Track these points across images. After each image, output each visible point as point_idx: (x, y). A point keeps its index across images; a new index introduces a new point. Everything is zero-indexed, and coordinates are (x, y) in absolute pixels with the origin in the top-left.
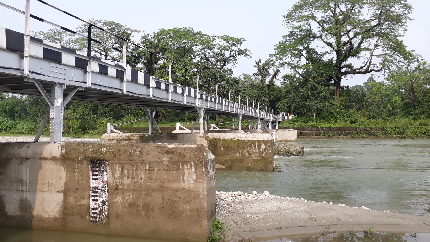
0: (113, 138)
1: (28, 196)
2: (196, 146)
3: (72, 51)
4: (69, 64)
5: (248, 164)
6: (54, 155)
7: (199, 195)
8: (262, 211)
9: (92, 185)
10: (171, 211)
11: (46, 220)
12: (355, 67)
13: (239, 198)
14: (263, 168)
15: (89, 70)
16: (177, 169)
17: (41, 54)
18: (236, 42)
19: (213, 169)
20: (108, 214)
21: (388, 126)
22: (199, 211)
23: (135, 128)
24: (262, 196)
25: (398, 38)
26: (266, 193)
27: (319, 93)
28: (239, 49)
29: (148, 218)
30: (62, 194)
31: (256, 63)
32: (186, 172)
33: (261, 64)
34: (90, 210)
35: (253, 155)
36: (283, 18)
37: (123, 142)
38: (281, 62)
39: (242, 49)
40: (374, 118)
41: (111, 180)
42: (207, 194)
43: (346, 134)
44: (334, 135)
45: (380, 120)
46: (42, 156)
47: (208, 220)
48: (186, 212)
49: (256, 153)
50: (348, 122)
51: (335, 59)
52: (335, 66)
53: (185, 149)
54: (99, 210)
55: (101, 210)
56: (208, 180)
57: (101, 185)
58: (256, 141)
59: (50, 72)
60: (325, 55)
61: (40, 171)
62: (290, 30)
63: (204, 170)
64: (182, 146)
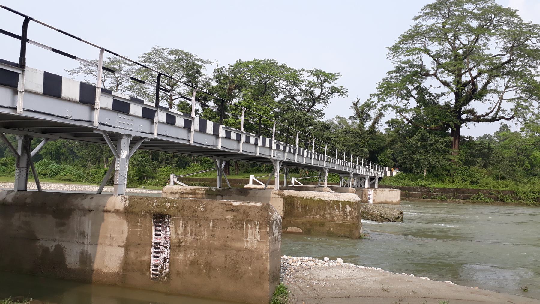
0: (176, 191)
1: (89, 249)
2: (261, 204)
3: (141, 102)
4: (137, 114)
5: (330, 229)
6: (117, 208)
7: (262, 256)
8: (331, 279)
9: (154, 241)
10: (233, 271)
11: (106, 274)
12: (479, 114)
13: (308, 264)
14: (347, 234)
15: (156, 120)
16: (241, 228)
17: (110, 106)
18: (330, 77)
19: (279, 230)
20: (169, 271)
21: (520, 190)
22: (261, 273)
23: (202, 179)
24: (333, 263)
25: (535, 78)
26: (340, 260)
27: (431, 145)
28: (333, 86)
29: (210, 277)
30: (123, 249)
31: (354, 104)
32: (250, 231)
33: (360, 105)
34: (151, 267)
35: (336, 219)
36: (388, 50)
37: (187, 196)
38: (385, 104)
39: (337, 86)
40: (503, 178)
41: (174, 236)
42: (271, 256)
43: (465, 198)
44: (450, 198)
45: (511, 183)
46: (105, 209)
47: (271, 283)
48: (249, 273)
49: (340, 216)
50: (468, 183)
51: (453, 102)
52: (454, 111)
53: (250, 207)
54: (160, 267)
55: (162, 267)
56: (273, 241)
57: (163, 241)
58: (340, 202)
59: (118, 123)
60: (441, 97)
61: (103, 224)
62: (396, 65)
63: (268, 230)
64: (247, 204)
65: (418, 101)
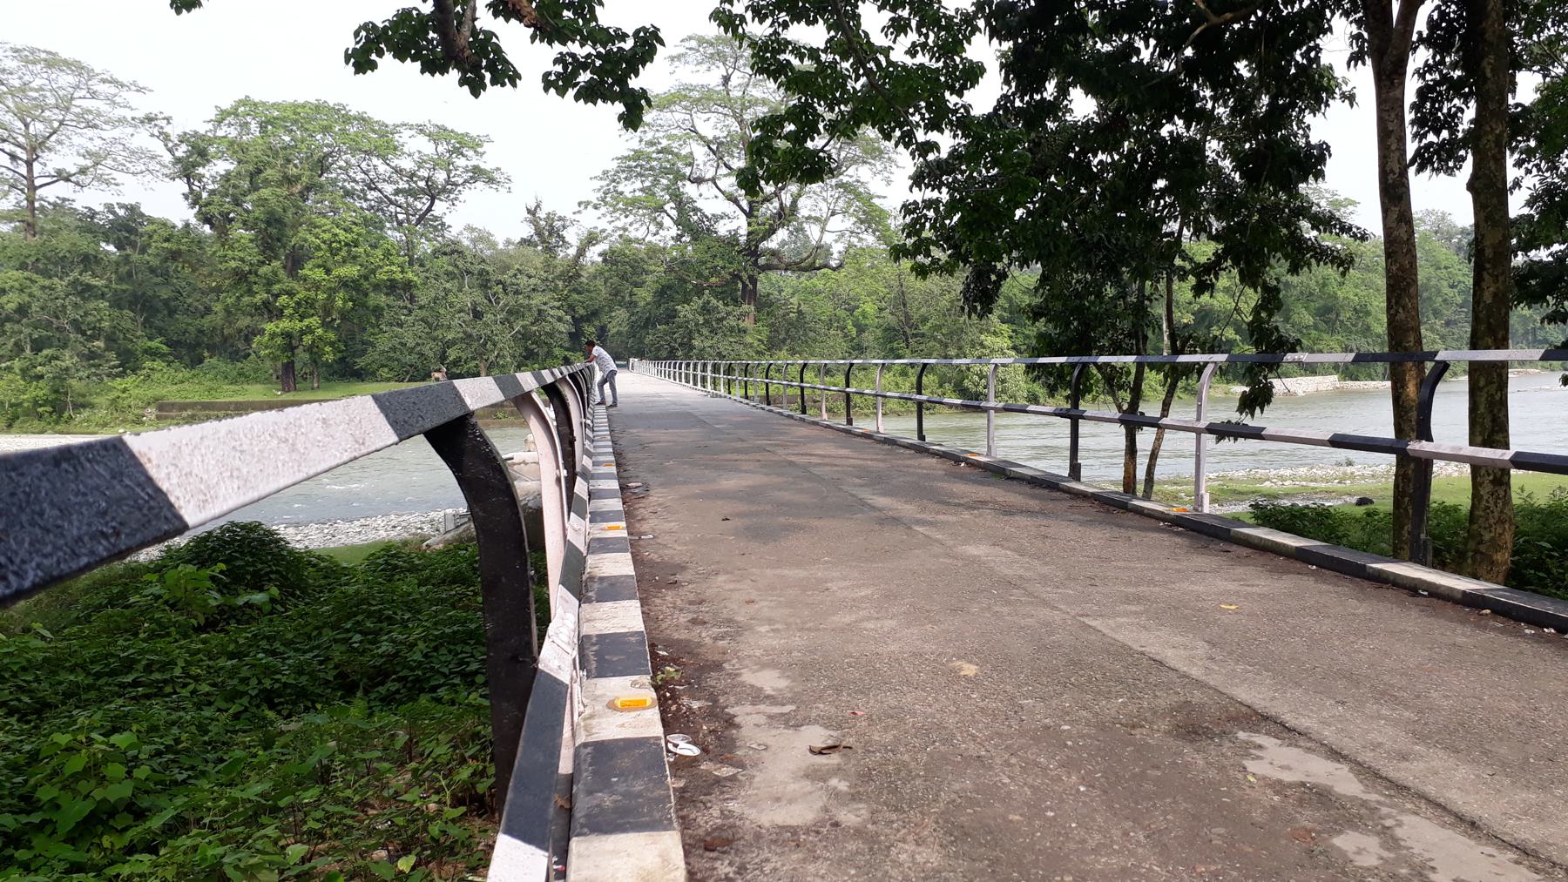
25: (876, 201)
31: (529, 211)
39: (483, 166)
51: (744, 231)
60: (726, 221)
62: (635, 145)
65: (677, 223)
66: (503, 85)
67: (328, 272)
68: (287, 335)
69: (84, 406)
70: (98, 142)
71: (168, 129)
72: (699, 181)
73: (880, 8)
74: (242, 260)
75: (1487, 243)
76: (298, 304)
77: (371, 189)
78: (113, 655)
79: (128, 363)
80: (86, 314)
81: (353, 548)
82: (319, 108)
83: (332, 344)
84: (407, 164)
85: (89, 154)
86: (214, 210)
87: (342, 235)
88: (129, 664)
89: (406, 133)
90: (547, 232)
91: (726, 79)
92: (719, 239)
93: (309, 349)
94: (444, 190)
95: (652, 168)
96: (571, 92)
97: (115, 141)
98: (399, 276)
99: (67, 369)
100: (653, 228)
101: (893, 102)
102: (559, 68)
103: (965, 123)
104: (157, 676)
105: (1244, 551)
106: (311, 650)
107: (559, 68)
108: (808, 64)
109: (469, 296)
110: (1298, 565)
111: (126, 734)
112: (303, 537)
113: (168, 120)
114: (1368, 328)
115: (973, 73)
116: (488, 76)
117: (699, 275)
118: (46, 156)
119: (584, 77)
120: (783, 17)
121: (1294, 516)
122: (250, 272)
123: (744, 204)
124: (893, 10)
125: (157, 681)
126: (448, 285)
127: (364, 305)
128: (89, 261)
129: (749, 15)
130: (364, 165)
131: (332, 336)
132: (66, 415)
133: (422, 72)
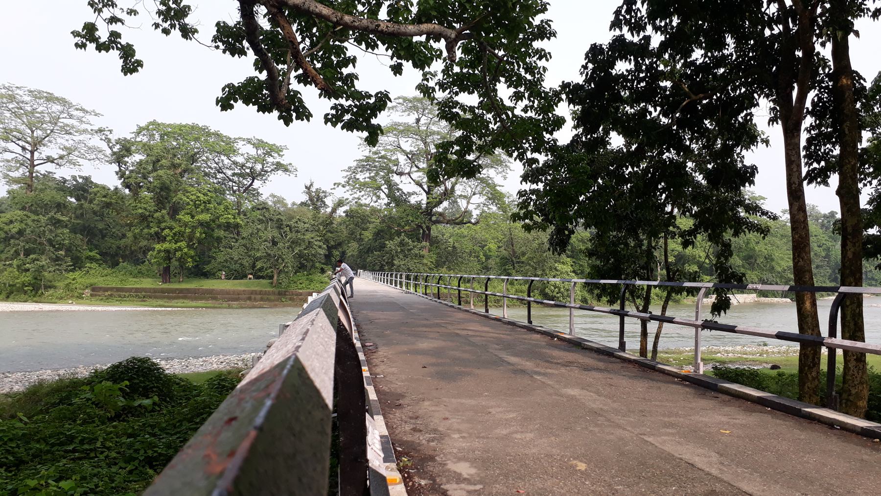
25: (498, 188)
31: (306, 187)
39: (282, 162)
51: (424, 202)
60: (415, 196)
62: (367, 153)
65: (388, 196)
66: (302, 120)
67: (193, 217)
68: (167, 251)
69: (50, 287)
70: (71, 142)
71: (110, 136)
72: (401, 174)
73: (508, 87)
74: (145, 209)
75: (849, 224)
76: (175, 234)
77: (219, 172)
78: (62, 433)
79: (77, 264)
80: (56, 236)
81: (198, 374)
82: (194, 127)
83: (192, 257)
84: (240, 160)
85: (65, 148)
86: (132, 181)
87: (202, 197)
88: (71, 439)
89: (241, 143)
90: (316, 199)
91: (418, 120)
92: (411, 206)
93: (179, 260)
94: (260, 174)
95: (375, 166)
96: (340, 125)
97: (80, 142)
98: (232, 221)
99: (43, 266)
100: (374, 198)
101: (514, 136)
102: (334, 112)
103: (553, 148)
104: (86, 447)
105: (727, 398)
106: (175, 434)
107: (334, 112)
108: (468, 116)
109: (271, 233)
110: (759, 407)
111: (69, 481)
112: (172, 367)
113: (111, 131)
114: (773, 268)
115: (559, 122)
116: (294, 115)
117: (399, 225)
118: (42, 148)
119: (347, 117)
120: (456, 89)
121: (737, 375)
122: (149, 216)
123: (425, 187)
124: (516, 87)
125: (87, 450)
126: (259, 227)
127: (211, 236)
128: (61, 207)
129: (437, 88)
130: (216, 159)
131: (192, 253)
132: (40, 292)
133: (258, 111)
